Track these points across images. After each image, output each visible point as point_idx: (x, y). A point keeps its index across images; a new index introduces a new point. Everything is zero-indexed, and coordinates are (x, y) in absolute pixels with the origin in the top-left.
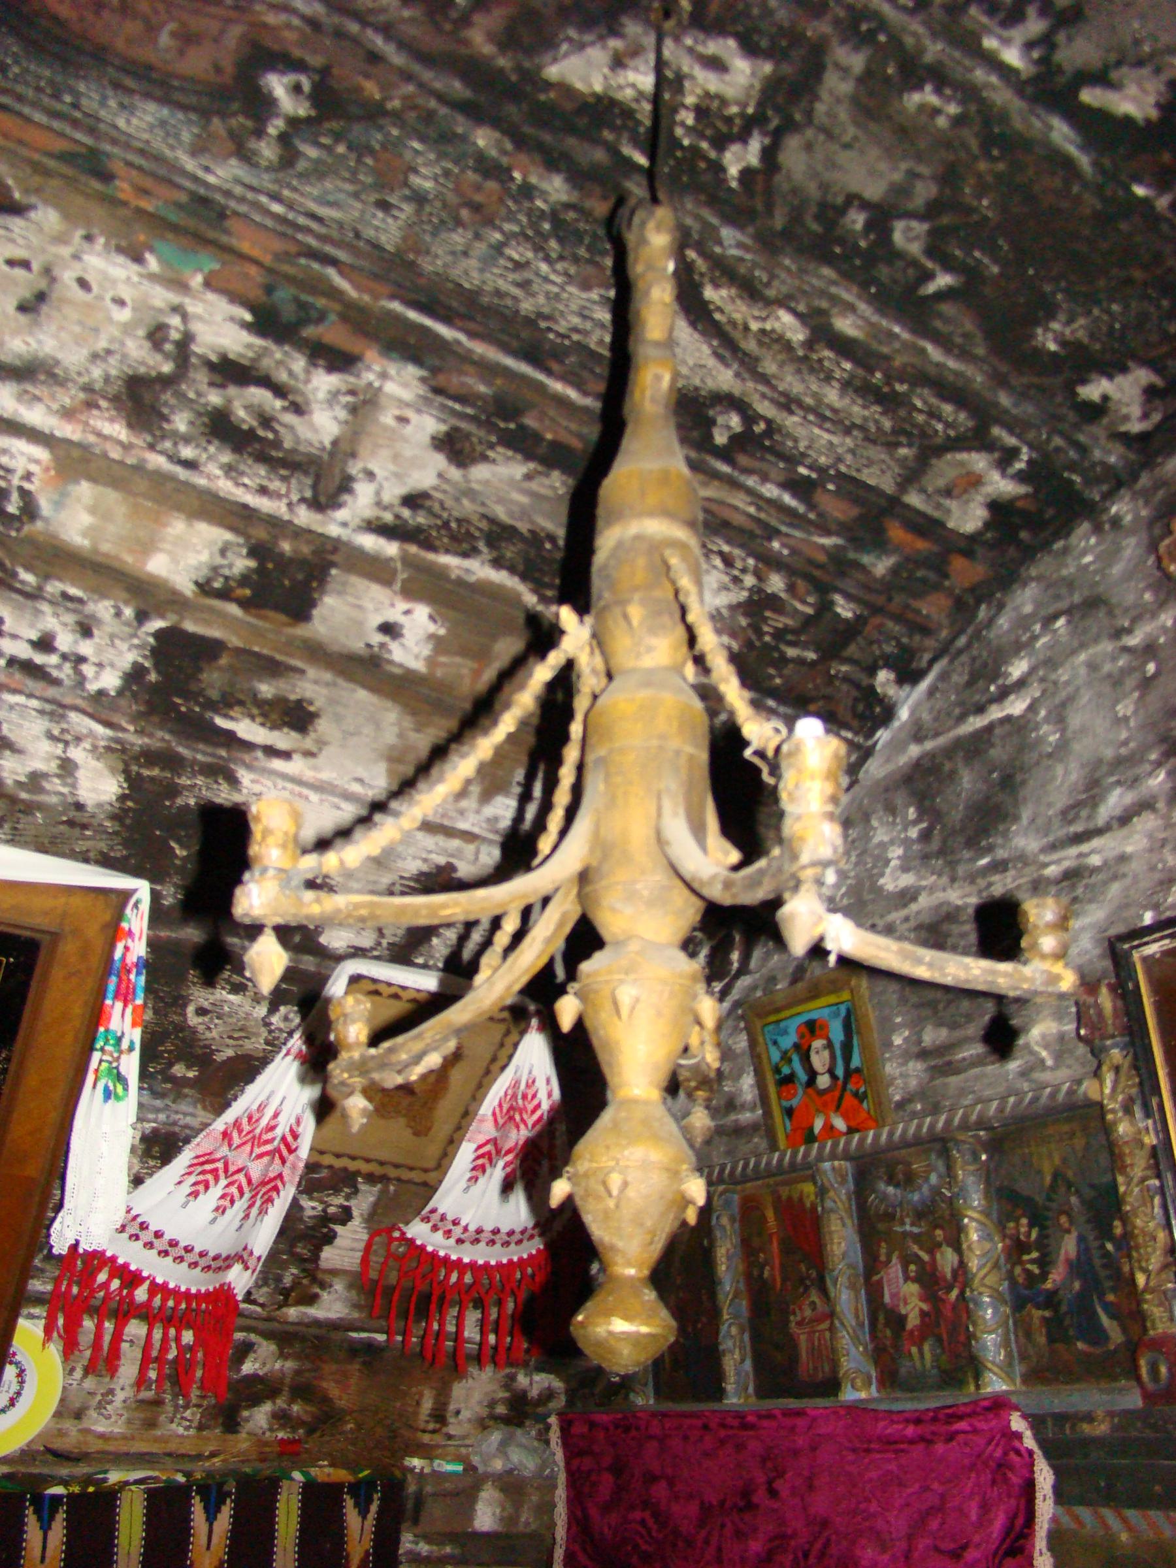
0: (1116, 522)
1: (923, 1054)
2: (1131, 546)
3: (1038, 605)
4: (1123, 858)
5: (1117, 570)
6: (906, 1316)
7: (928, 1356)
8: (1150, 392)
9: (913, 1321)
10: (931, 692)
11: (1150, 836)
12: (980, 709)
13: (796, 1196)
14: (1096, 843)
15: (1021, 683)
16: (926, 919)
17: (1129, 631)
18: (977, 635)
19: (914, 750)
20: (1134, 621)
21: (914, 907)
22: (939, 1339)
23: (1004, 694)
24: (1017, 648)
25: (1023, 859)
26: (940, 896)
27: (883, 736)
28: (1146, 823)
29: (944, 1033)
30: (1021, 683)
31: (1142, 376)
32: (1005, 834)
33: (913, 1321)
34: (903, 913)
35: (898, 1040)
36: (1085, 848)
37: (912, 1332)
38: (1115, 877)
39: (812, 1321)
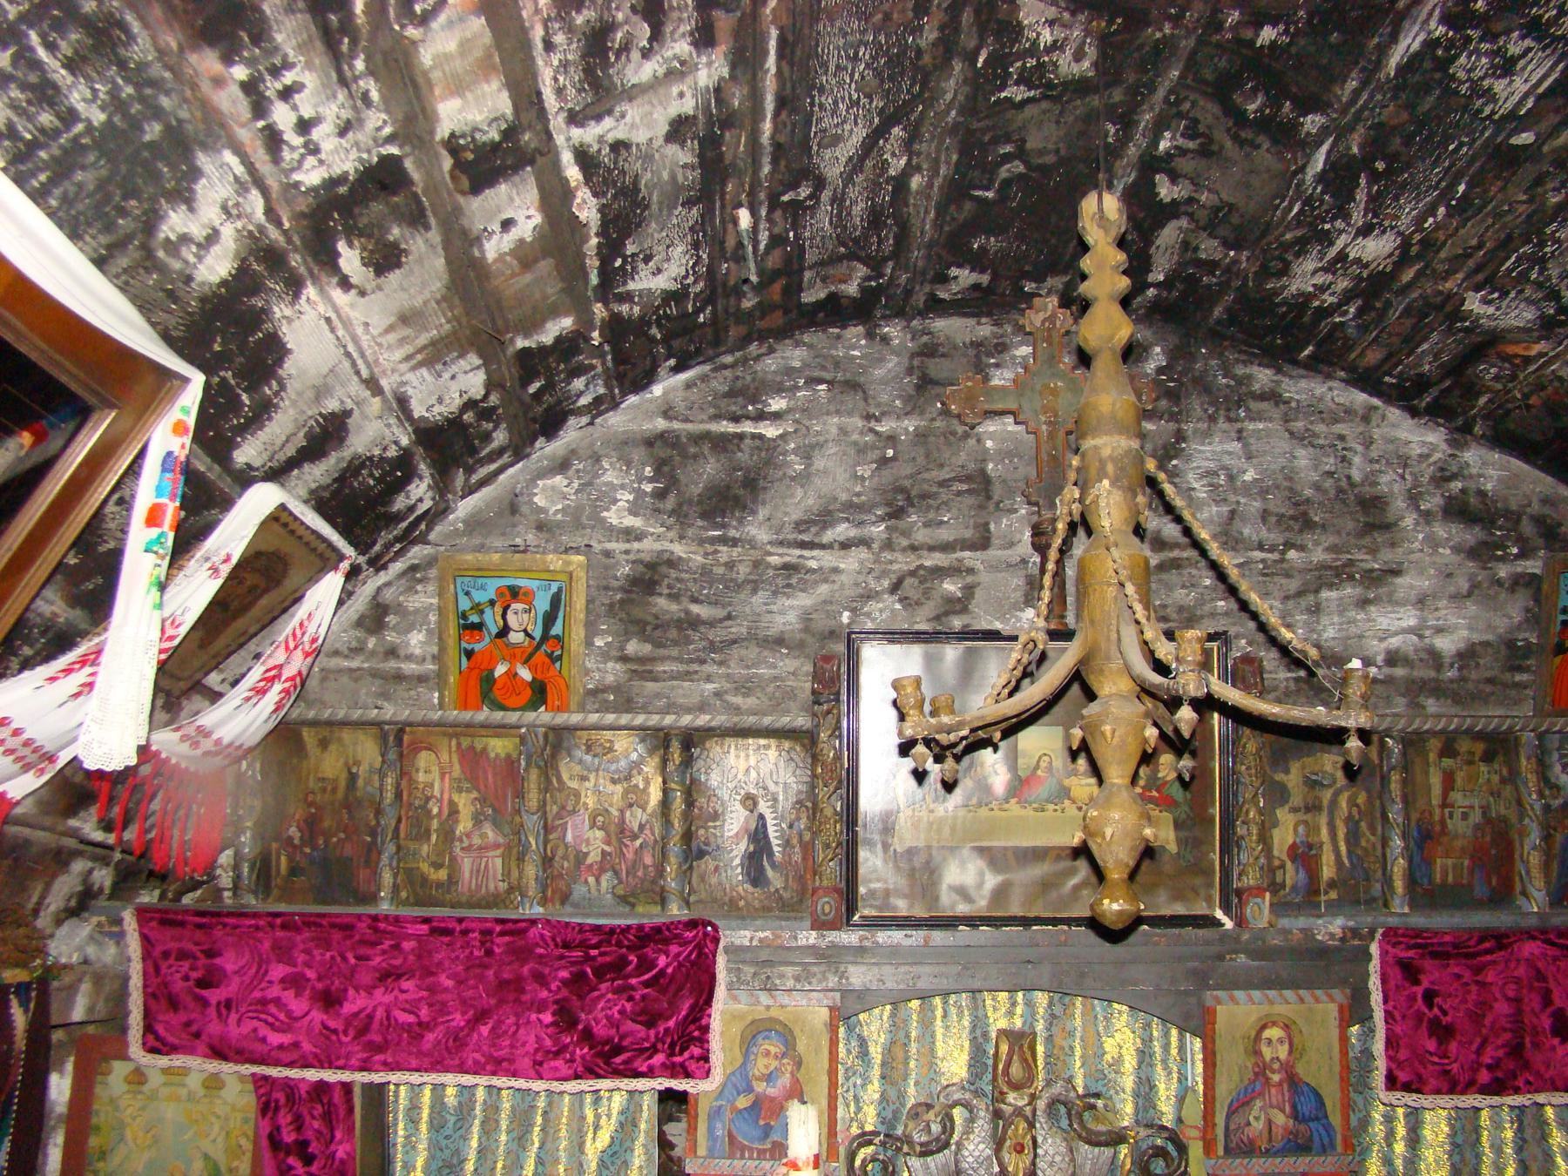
0: (885, 339)
1: (624, 659)
2: (892, 363)
3: (806, 365)
4: (836, 570)
5: (879, 373)
6: (586, 854)
7: (604, 884)
10: (689, 385)
11: (861, 563)
12: (736, 419)
13: (479, 747)
14: (815, 553)
15: (777, 416)
16: (647, 558)
17: (878, 420)
18: (745, 361)
19: (661, 424)
20: (883, 414)
21: (636, 545)
22: (616, 873)
23: (760, 417)
24: (779, 390)
25: (752, 543)
26: (667, 545)
27: (633, 399)
28: (862, 553)
29: (647, 649)
30: (777, 416)
32: (741, 521)
34: (627, 546)
35: (599, 642)
36: (806, 553)
37: (591, 865)
38: (826, 581)
39: (480, 848)
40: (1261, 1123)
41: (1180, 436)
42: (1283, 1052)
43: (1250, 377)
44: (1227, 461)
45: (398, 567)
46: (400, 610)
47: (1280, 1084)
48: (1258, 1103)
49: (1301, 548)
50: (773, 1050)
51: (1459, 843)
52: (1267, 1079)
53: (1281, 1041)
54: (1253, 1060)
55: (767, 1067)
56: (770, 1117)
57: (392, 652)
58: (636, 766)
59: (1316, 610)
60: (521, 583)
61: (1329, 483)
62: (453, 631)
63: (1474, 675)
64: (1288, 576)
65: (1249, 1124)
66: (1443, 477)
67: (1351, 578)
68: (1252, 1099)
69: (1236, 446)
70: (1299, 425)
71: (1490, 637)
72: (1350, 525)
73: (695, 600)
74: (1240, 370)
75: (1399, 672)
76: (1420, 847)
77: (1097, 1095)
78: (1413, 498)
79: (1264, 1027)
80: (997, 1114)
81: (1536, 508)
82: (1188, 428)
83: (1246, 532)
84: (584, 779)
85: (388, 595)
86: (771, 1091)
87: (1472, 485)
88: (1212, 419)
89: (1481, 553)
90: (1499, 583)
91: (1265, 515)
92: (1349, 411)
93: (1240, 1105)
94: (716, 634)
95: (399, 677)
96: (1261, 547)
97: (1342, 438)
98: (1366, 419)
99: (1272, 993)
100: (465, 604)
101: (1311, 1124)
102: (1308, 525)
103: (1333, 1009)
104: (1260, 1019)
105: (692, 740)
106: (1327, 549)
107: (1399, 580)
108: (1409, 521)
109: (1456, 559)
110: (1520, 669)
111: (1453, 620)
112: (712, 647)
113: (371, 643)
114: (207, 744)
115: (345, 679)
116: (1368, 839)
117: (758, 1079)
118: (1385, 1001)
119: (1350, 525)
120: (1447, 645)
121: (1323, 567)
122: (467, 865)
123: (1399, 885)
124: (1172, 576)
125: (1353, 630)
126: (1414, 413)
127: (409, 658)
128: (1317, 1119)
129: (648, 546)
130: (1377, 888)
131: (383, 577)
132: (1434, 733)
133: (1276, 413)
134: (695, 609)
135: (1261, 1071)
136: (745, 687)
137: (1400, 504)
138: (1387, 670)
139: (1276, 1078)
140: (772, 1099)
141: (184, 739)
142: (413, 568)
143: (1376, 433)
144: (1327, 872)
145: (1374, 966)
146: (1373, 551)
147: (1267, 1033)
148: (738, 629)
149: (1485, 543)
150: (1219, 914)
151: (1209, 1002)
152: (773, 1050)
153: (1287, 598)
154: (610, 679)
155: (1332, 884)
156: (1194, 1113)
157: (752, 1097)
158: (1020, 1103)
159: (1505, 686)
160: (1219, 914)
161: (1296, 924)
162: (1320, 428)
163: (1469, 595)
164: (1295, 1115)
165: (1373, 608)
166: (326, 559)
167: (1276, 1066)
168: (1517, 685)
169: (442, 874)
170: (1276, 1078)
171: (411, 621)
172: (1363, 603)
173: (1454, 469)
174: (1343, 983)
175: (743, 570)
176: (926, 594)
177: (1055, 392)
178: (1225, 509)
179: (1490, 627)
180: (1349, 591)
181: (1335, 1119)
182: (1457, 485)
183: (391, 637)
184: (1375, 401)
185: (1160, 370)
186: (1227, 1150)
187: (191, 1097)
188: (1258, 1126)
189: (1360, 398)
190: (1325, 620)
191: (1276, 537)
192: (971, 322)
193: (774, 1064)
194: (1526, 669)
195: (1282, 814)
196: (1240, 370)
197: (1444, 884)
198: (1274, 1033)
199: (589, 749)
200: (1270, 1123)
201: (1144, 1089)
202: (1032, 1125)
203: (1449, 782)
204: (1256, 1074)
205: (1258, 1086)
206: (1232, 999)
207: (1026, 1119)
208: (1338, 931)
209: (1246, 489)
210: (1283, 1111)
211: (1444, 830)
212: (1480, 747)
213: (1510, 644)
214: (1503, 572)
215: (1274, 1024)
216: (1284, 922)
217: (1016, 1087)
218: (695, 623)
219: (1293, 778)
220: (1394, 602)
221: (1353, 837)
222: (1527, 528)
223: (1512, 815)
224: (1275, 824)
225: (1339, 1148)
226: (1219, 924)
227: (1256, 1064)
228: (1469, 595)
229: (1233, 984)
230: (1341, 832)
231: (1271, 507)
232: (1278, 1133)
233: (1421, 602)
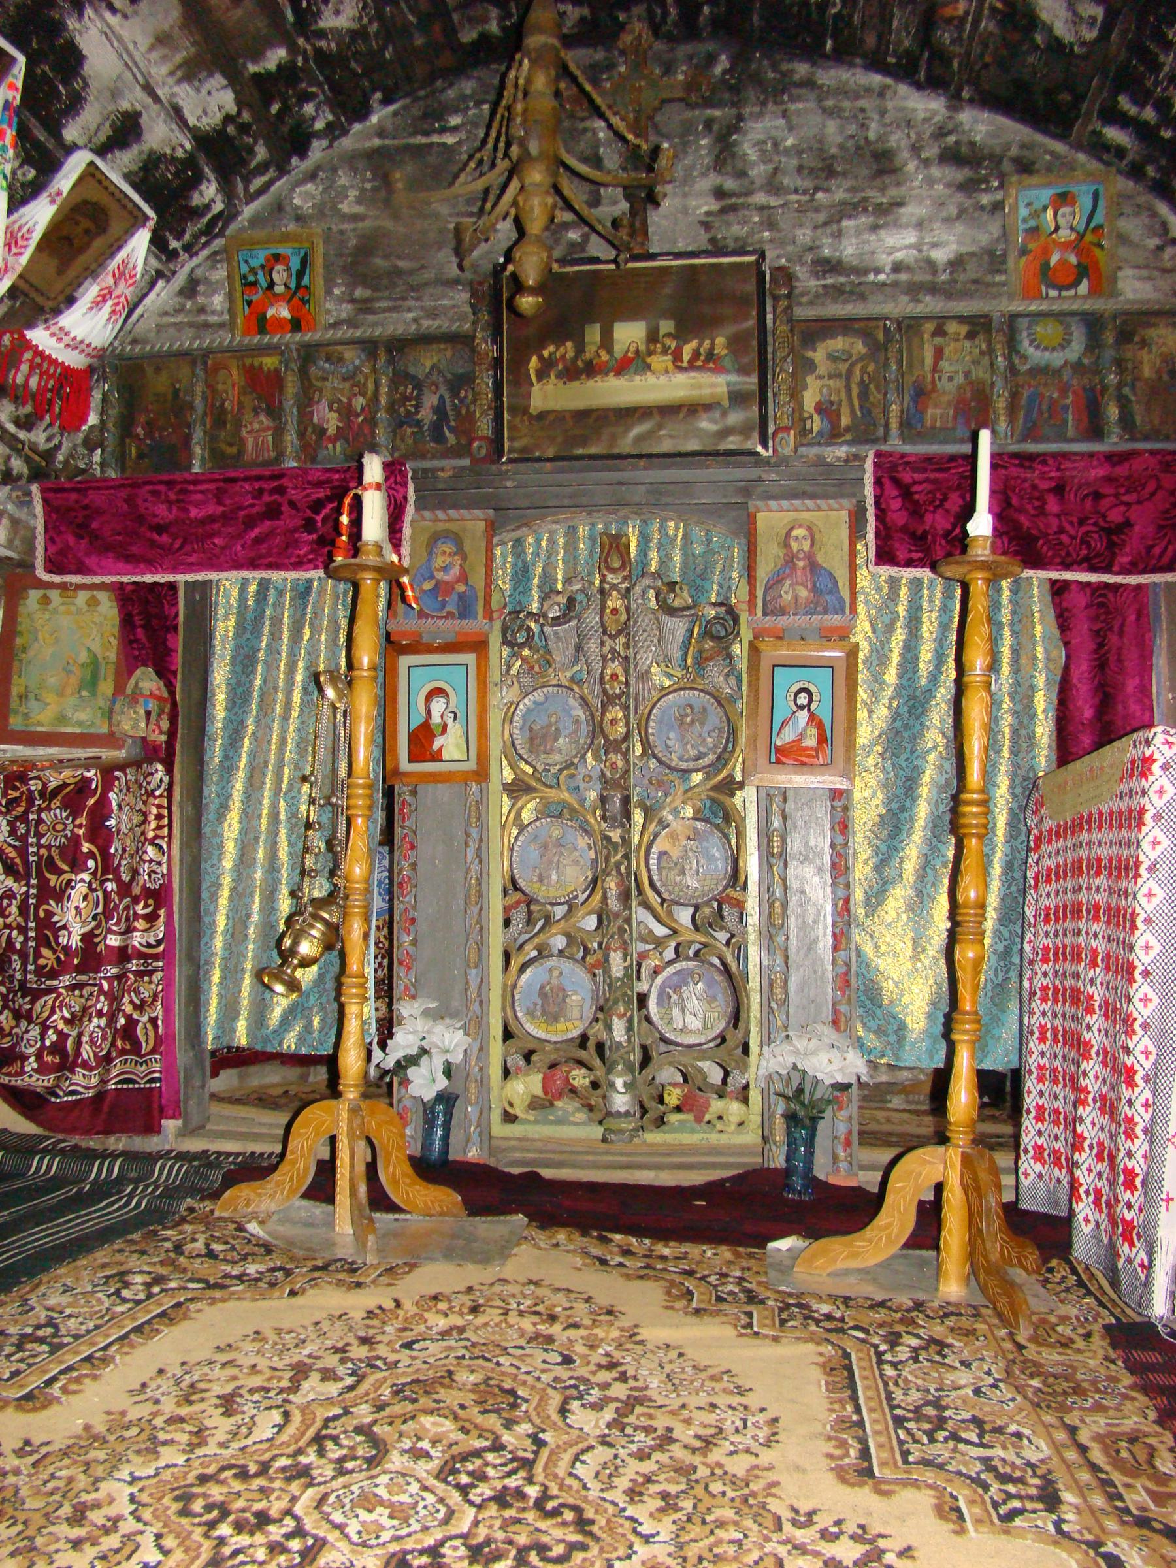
1: (353, 301)
3: (474, 92)
8: (582, 20)
9: (332, 431)
10: (395, 114)
12: (427, 134)
15: (455, 129)
18: (433, 93)
19: (377, 142)
23: (443, 130)
24: (456, 111)
25: (437, 216)
26: (378, 223)
27: (357, 127)
29: (368, 293)
30: (455, 129)
31: (586, 12)
33: (332, 431)
35: (336, 292)
41: (740, 118)
42: (806, 546)
43: (792, 71)
44: (774, 133)
45: (205, 253)
46: (207, 281)
49: (827, 190)
51: (945, 399)
57: (202, 310)
58: (357, 369)
59: (839, 235)
60: (281, 251)
61: (850, 144)
62: (238, 288)
63: (962, 277)
64: (817, 210)
66: (941, 133)
67: (865, 210)
69: (781, 122)
70: (830, 103)
71: (974, 249)
72: (865, 172)
73: (399, 258)
74: (785, 67)
75: (903, 277)
76: (916, 402)
78: (915, 149)
81: (1014, 151)
82: (747, 111)
83: (786, 181)
84: (325, 379)
85: (199, 272)
86: (447, 578)
87: (964, 139)
88: (763, 104)
89: (968, 187)
90: (982, 208)
91: (800, 169)
92: (868, 90)
93: (776, 581)
94: (414, 280)
95: (206, 326)
96: (796, 191)
97: (863, 110)
98: (881, 95)
99: (796, 503)
100: (245, 269)
102: (831, 173)
103: (844, 514)
105: (398, 346)
106: (847, 190)
107: (903, 210)
108: (911, 166)
109: (948, 192)
110: (998, 271)
111: (945, 237)
112: (412, 288)
113: (189, 305)
114: (67, 340)
115: (172, 330)
116: (875, 396)
119: (865, 172)
120: (940, 256)
121: (844, 203)
122: (250, 441)
123: (894, 424)
124: (731, 217)
125: (867, 248)
126: (919, 86)
127: (213, 312)
129: (367, 224)
130: (881, 430)
131: (195, 261)
132: (928, 318)
133: (812, 96)
134: (401, 264)
135: (790, 560)
136: (433, 314)
137: (906, 154)
138: (893, 277)
139: (801, 564)
141: (53, 335)
142: (215, 253)
143: (890, 105)
144: (845, 421)
146: (883, 190)
148: (429, 275)
149: (971, 180)
150: (759, 449)
153: (816, 228)
154: (344, 315)
155: (848, 429)
159: (988, 285)
160: (759, 449)
161: (814, 451)
162: (846, 104)
163: (959, 217)
164: (814, 589)
165: (882, 232)
166: (139, 220)
168: (995, 284)
169: (233, 450)
170: (801, 564)
171: (213, 289)
172: (875, 228)
173: (950, 126)
175: (432, 235)
176: (557, 241)
177: (640, 89)
178: (770, 167)
179: (974, 241)
180: (864, 220)
181: (845, 594)
182: (951, 139)
183: (201, 300)
184: (889, 81)
185: (724, 72)
186: (765, 614)
187: (79, 612)
189: (877, 79)
190: (845, 242)
191: (808, 184)
192: (591, 51)
194: (1005, 272)
195: (809, 379)
196: (785, 67)
197: (933, 427)
199: (328, 360)
203: (939, 353)
209: (787, 151)
211: (934, 389)
212: (964, 329)
213: (991, 253)
214: (985, 199)
216: (802, 450)
218: (398, 273)
219: (819, 355)
220: (897, 225)
221: (864, 394)
222: (1007, 166)
223: (987, 376)
224: (805, 387)
228: (959, 217)
229: (768, 497)
230: (855, 391)
231: (805, 163)
233: (920, 225)
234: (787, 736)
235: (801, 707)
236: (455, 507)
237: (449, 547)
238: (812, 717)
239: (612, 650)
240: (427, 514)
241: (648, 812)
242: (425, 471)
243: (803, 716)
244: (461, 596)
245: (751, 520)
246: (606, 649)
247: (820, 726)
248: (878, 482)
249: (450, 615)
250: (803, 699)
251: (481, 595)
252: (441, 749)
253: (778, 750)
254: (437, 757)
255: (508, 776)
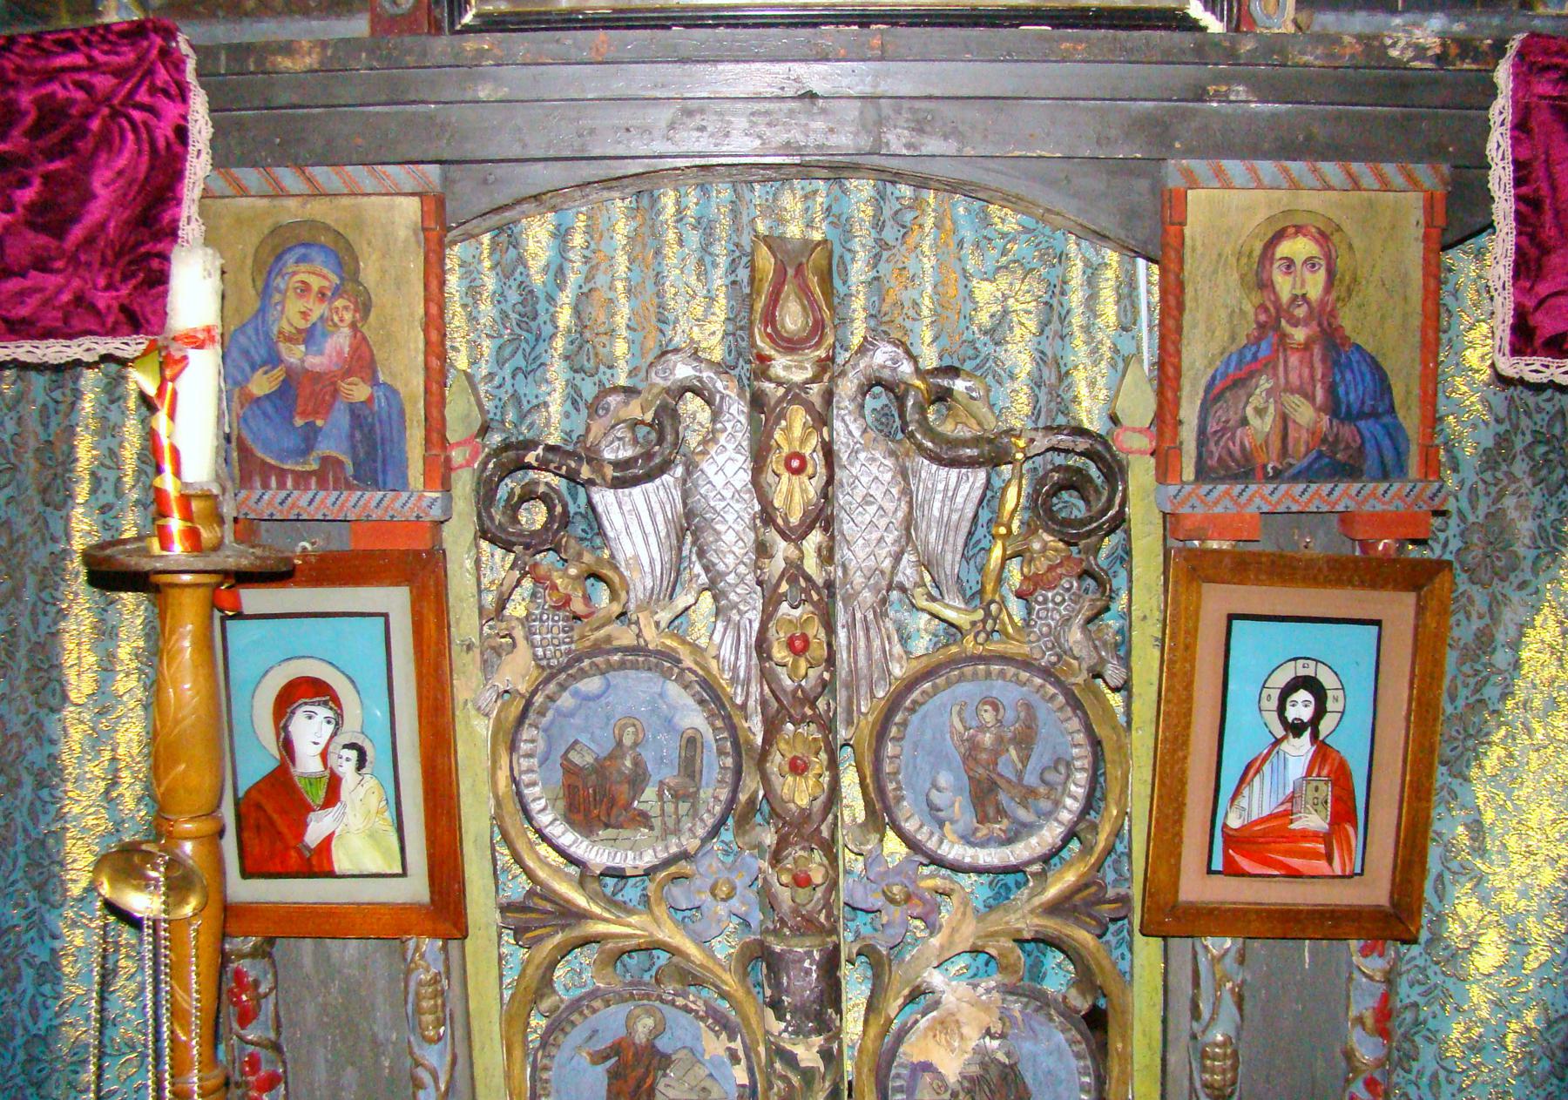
40: (1269, 419)
42: (1314, 286)
47: (1307, 346)
48: (1265, 383)
50: (316, 283)
52: (1283, 336)
53: (1310, 263)
54: (1257, 297)
55: (305, 315)
56: (316, 413)
65: (1244, 422)
68: (1251, 375)
77: (953, 372)
79: (1279, 236)
80: (757, 402)
86: (316, 362)
99: (1297, 167)
101: (1362, 424)
104: (1270, 219)
117: (290, 339)
118: (1518, 182)
128: (1374, 415)
135: (1272, 321)
140: (315, 377)
145: (1501, 110)
147: (1285, 249)
151: (1174, 181)
152: (316, 283)
156: (1139, 405)
157: (279, 373)
158: (798, 377)
164: (1334, 407)
167: (1301, 312)
170: (1299, 335)
174: (1432, 153)
181: (1410, 419)
186: (1202, 473)
188: (1262, 426)
193: (318, 310)
198: (1299, 248)
200: (1284, 419)
201: (1050, 376)
202: (822, 419)
204: (1261, 326)
205: (1264, 349)
206: (1219, 173)
207: (809, 408)
208: (1433, 43)
210: (1310, 398)
215: (1299, 230)
217: (791, 345)
225: (1414, 469)
226: (1193, 26)
227: (1262, 307)
232: (1300, 441)
234: (1260, 802)
235: (1296, 729)
236: (333, 160)
237: (319, 274)
238: (1323, 753)
239: (794, 571)
240: (251, 177)
241: (878, 964)
242: (239, 52)
243: (1299, 750)
244: (357, 414)
245: (1170, 209)
246: (777, 565)
247: (1341, 777)
248: (1521, 128)
249: (328, 473)
250: (1301, 707)
251: (416, 413)
252: (328, 840)
253: (1231, 839)
254: (318, 864)
255: (517, 887)
